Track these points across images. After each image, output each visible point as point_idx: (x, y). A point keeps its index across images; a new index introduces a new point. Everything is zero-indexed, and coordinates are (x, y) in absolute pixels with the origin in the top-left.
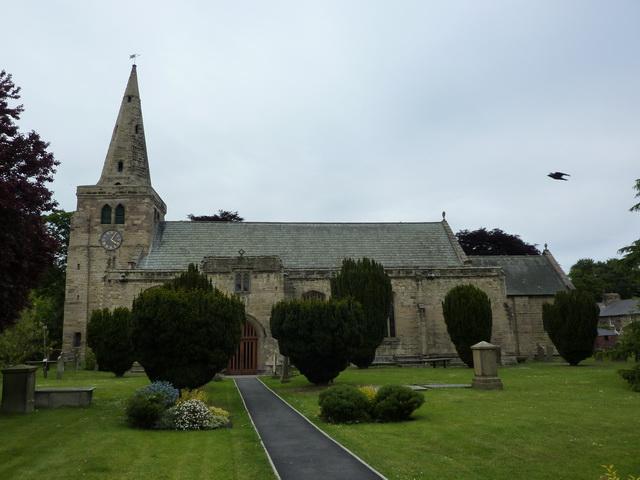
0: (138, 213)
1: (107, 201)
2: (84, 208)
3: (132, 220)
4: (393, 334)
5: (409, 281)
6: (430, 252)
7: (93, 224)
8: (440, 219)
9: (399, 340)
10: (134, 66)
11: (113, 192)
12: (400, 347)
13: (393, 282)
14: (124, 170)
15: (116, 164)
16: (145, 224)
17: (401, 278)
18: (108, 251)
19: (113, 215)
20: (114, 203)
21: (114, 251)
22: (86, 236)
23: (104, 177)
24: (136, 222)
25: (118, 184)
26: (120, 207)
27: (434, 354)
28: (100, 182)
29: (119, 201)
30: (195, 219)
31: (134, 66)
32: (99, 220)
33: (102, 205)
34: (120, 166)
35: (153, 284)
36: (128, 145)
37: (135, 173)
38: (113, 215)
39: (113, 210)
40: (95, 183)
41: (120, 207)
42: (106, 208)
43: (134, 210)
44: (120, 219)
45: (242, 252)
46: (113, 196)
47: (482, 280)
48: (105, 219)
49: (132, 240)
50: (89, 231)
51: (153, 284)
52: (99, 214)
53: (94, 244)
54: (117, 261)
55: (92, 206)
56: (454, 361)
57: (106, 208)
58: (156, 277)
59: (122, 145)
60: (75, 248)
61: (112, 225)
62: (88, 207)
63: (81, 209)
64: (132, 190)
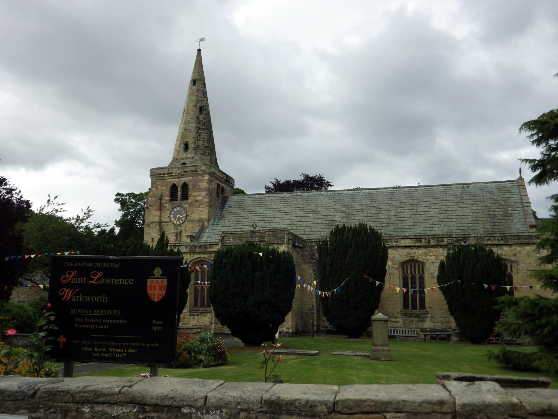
0: (199, 189)
1: (175, 181)
2: (156, 188)
3: (194, 196)
4: (423, 306)
5: (441, 250)
6: (495, 216)
7: (163, 202)
8: (516, 177)
9: (427, 313)
10: (199, 50)
11: (179, 172)
12: (428, 319)
13: (390, 251)
14: (189, 151)
15: (183, 146)
16: (205, 200)
17: (432, 247)
18: (175, 225)
19: (179, 193)
20: (180, 182)
21: (180, 225)
22: (158, 213)
23: (175, 160)
24: (198, 198)
25: (184, 164)
26: (185, 186)
27: (430, 329)
28: (171, 164)
29: (183, 180)
30: (282, 187)
31: (199, 50)
32: (168, 198)
33: (172, 183)
34: (186, 147)
35: (196, 256)
36: (192, 126)
37: (199, 153)
38: (179, 193)
39: (179, 189)
40: (166, 164)
41: (185, 186)
42: (174, 188)
43: (197, 188)
44: (185, 197)
45: (254, 226)
46: (179, 176)
47: (528, 248)
48: (173, 197)
49: (195, 216)
50: (161, 208)
51: (196, 256)
52: (168, 193)
53: (164, 220)
54: (183, 234)
55: (163, 186)
56: (454, 338)
57: (174, 188)
58: (198, 250)
59: (188, 128)
60: (149, 224)
61: (179, 202)
62: (159, 187)
63: (154, 189)
64: (194, 169)
